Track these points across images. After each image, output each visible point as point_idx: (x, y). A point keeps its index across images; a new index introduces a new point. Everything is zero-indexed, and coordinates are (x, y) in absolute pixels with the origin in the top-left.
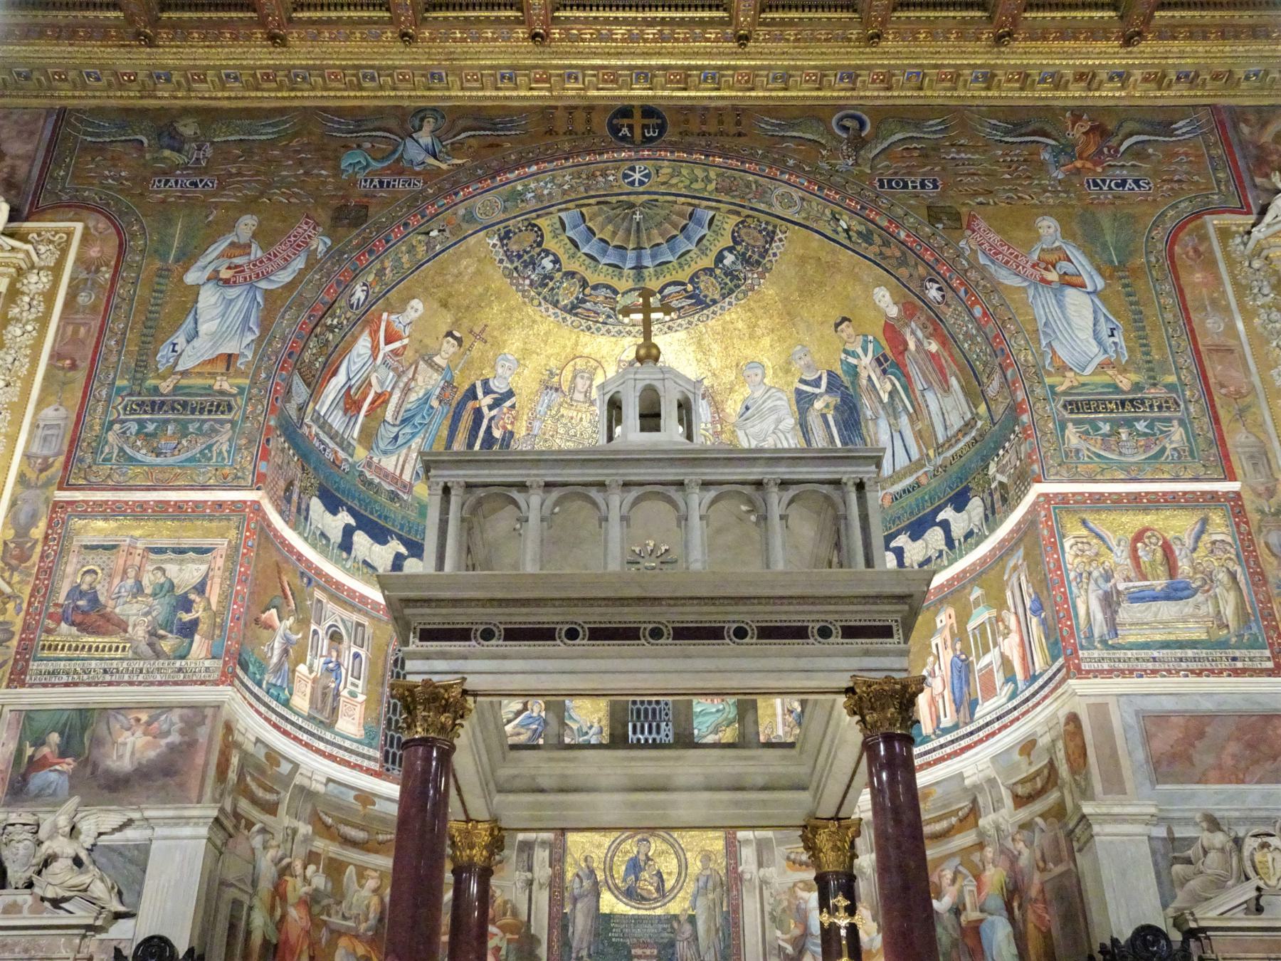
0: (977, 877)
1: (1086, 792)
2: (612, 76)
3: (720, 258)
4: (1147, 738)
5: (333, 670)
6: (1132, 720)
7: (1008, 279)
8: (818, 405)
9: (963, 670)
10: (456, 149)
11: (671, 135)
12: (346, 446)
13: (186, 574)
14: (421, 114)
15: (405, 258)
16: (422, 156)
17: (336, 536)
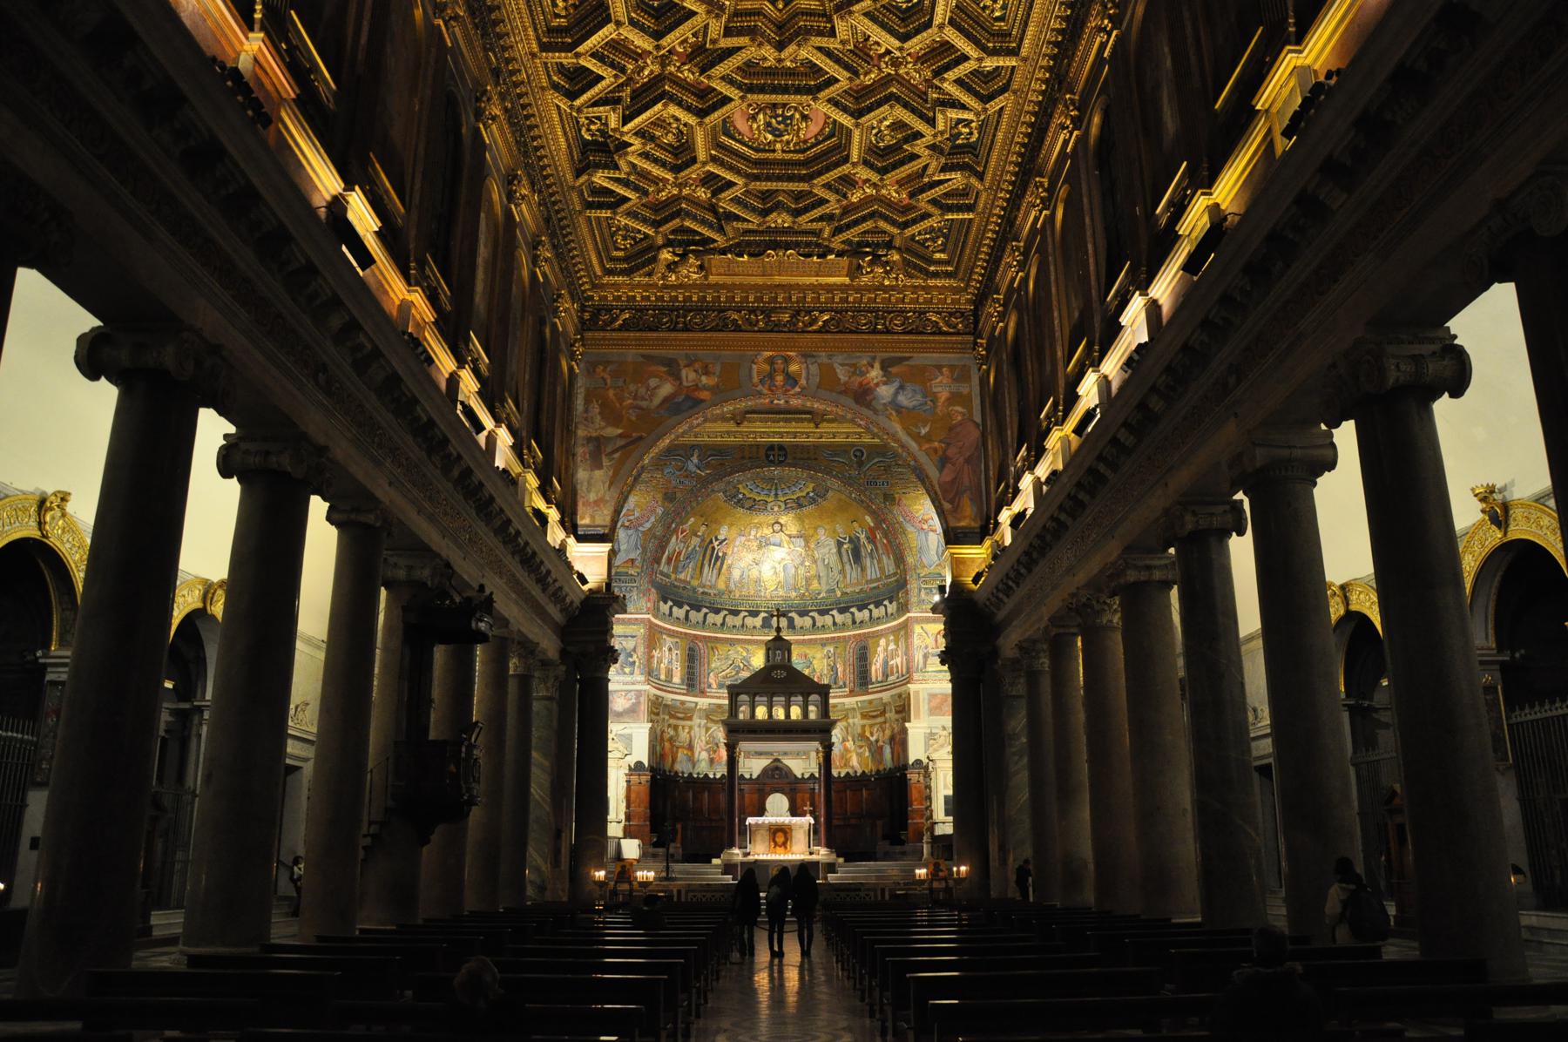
0: (884, 731)
1: (909, 721)
2: (768, 434)
3: (808, 493)
4: (930, 701)
5: (670, 662)
6: (926, 697)
7: (910, 528)
8: (845, 546)
9: (886, 663)
10: (708, 466)
11: (789, 461)
12: (668, 576)
13: (629, 644)
14: (693, 447)
15: (689, 509)
16: (694, 469)
17: (667, 613)
